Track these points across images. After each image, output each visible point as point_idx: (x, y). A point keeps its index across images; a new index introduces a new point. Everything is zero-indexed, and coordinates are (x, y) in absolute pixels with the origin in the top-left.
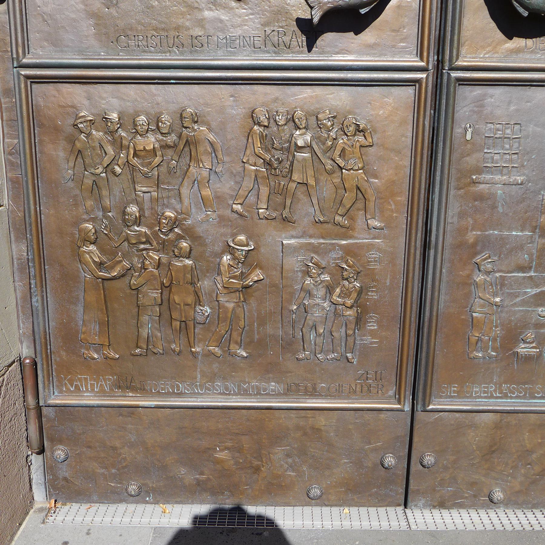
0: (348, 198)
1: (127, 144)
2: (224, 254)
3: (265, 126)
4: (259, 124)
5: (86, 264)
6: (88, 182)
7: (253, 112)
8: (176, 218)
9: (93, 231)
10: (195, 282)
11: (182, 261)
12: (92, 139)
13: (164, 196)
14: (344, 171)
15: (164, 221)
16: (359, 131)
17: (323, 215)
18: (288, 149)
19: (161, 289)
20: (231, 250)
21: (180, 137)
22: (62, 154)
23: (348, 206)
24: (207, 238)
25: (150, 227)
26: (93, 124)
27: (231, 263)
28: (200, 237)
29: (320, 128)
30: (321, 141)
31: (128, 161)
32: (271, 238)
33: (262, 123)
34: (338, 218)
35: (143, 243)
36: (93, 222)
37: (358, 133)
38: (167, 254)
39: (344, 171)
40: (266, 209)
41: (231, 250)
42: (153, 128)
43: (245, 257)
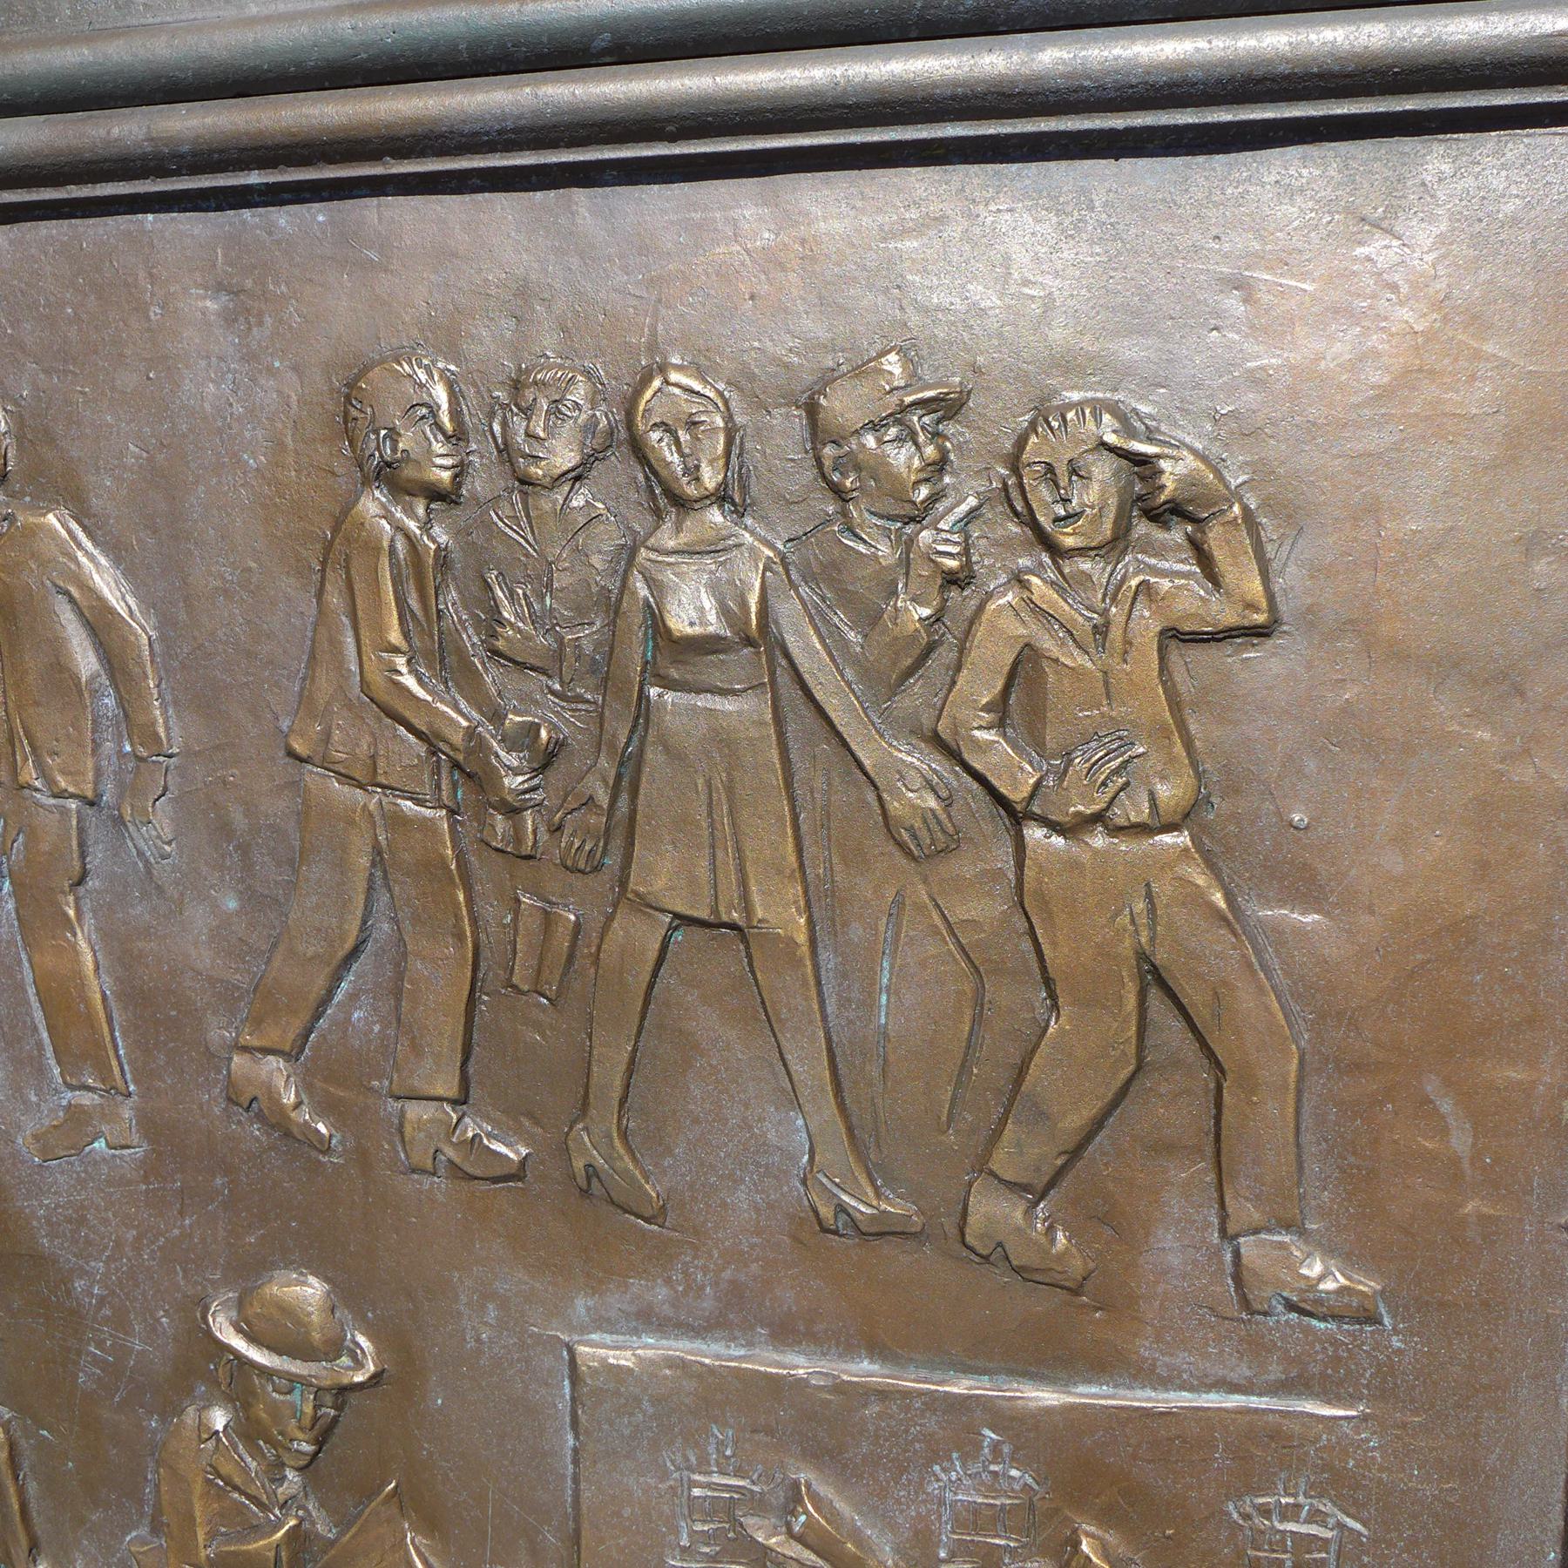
0: (1078, 1048)
3: (435, 494)
4: (391, 476)
7: (350, 393)
14: (1035, 834)
16: (1155, 516)
17: (879, 1174)
18: (604, 671)
23: (1075, 1121)
24: (83, 1273)
28: (39, 1260)
29: (838, 492)
30: (847, 599)
32: (492, 1312)
33: (409, 472)
34: (994, 1211)
37: (1142, 528)
39: (1035, 834)
40: (455, 1103)
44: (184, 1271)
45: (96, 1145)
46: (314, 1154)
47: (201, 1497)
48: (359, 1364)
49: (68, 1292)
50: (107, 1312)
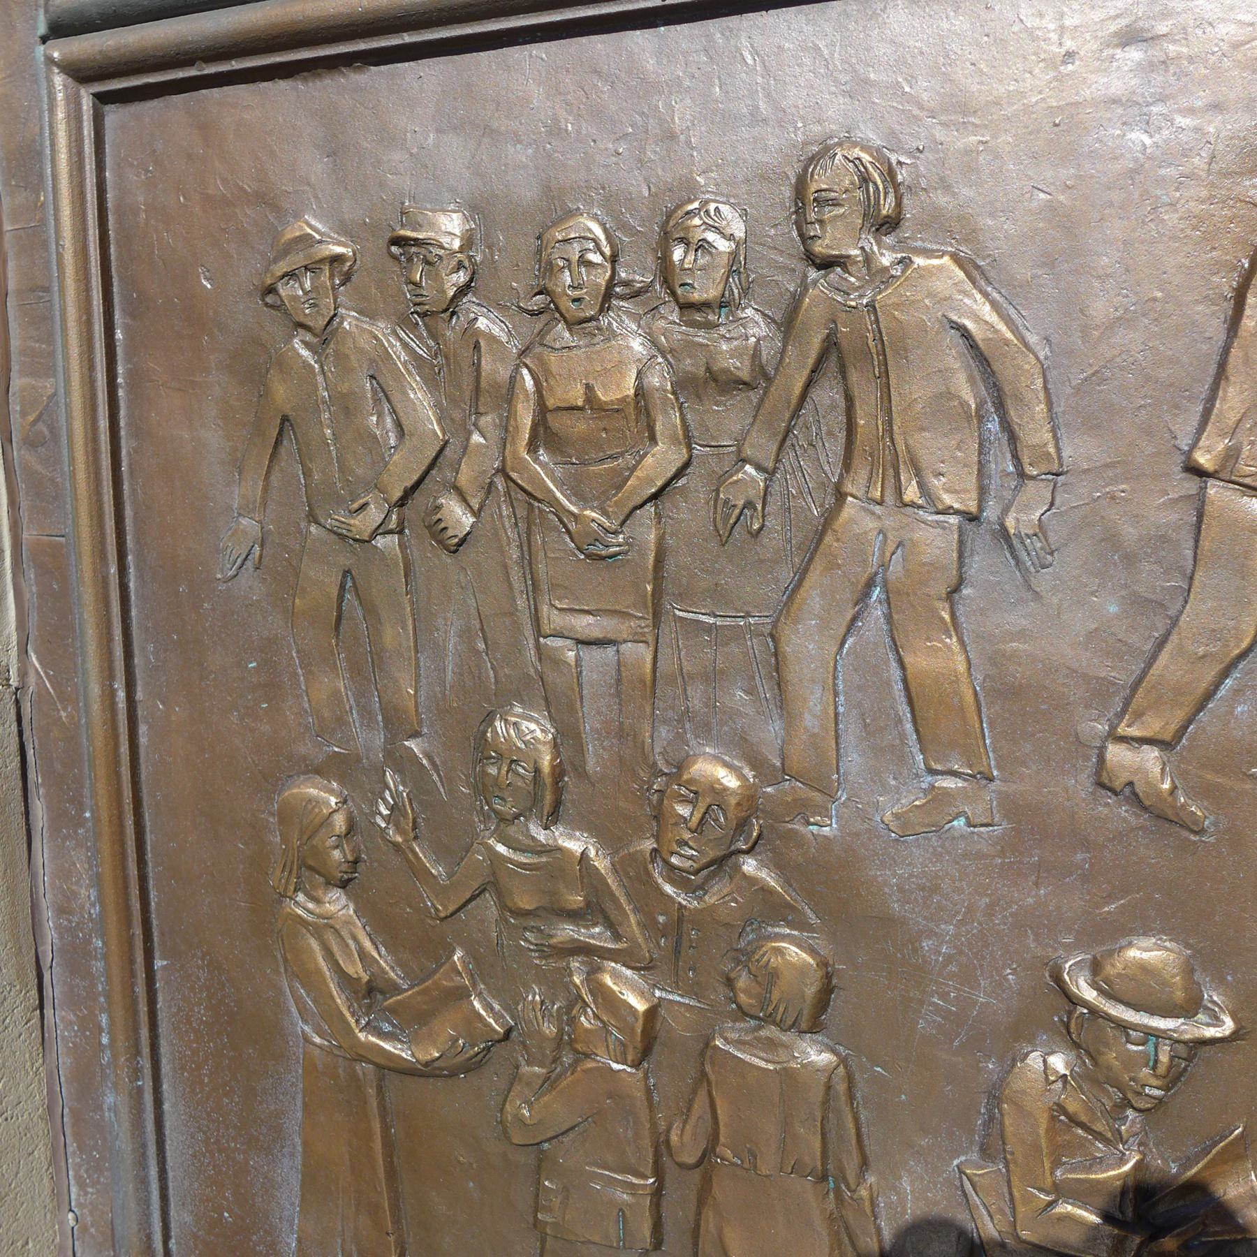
1: (504, 373)
2: (1031, 1040)
5: (310, 979)
6: (322, 579)
8: (750, 801)
9: (339, 822)
10: (842, 1170)
11: (771, 1045)
12: (341, 358)
13: (687, 667)
15: (683, 810)
19: (658, 1172)
20: (1078, 1028)
21: (788, 322)
22: (214, 439)
24: (931, 934)
25: (609, 838)
26: (347, 279)
27: (1072, 1107)
31: (502, 471)
35: (574, 916)
36: (342, 782)
38: (695, 990)
41: (1078, 1028)
42: (640, 279)
43: (1172, 1079)
44: (1036, 935)
45: (955, 823)
46: (1185, 834)
47: (1047, 1131)
48: (1217, 1022)
49: (915, 950)
50: (953, 968)
